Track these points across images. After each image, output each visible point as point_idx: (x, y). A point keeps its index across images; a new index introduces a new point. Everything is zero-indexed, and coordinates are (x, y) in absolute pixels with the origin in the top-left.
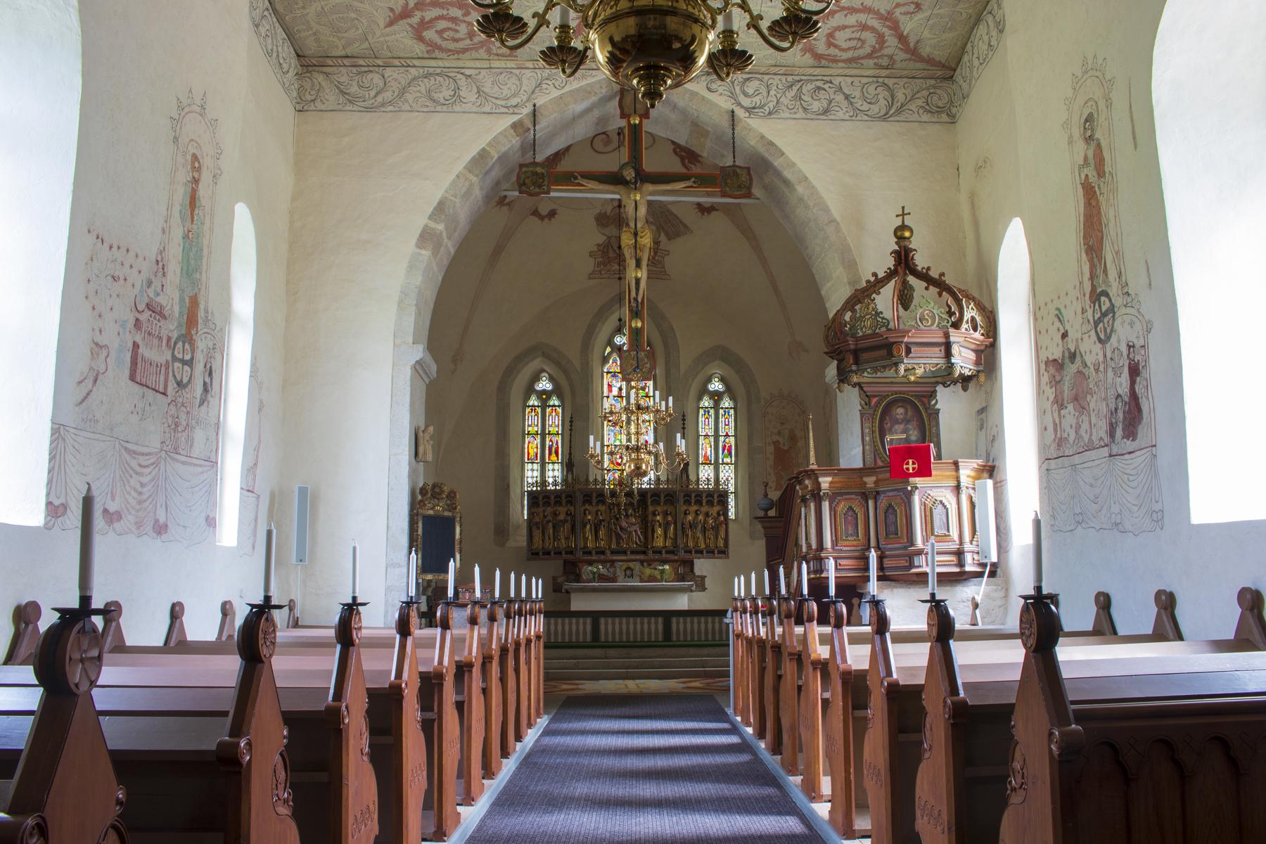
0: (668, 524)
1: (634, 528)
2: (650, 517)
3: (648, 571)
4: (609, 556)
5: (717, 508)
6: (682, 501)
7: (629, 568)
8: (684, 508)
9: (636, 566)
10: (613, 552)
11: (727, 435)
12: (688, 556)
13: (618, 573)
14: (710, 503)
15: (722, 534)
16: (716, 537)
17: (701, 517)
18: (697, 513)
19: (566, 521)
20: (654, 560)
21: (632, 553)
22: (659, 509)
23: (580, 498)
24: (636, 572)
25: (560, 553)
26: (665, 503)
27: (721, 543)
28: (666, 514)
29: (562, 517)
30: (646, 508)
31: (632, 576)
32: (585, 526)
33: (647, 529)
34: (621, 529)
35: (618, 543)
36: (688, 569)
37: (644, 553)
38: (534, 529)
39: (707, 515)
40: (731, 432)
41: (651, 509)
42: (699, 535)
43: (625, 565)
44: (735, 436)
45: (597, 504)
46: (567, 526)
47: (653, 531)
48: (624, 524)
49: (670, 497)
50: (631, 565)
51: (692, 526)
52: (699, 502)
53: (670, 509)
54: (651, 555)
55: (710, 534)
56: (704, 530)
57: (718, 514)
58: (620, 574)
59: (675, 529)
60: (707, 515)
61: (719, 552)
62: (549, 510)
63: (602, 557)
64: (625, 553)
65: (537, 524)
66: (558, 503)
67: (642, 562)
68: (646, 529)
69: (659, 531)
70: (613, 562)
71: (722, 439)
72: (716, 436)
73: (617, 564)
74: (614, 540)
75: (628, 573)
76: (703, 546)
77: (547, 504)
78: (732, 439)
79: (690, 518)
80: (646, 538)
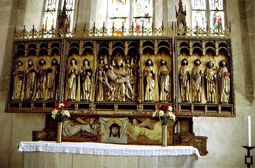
0: (162, 75)
1: (122, 80)
2: (143, 68)
3: (137, 130)
4: (93, 110)
5: (217, 60)
6: (179, 50)
7: (115, 125)
8: (181, 58)
9: (124, 123)
10: (100, 106)
11: (217, 10)
12: (186, 113)
13: (103, 130)
14: (211, 53)
15: (227, 88)
16: (219, 92)
17: (202, 68)
18: (196, 64)
19: (50, 71)
20: (145, 117)
21: (121, 107)
22: (153, 58)
23: (66, 48)
24: (124, 130)
25: (40, 105)
26: (160, 52)
27: (225, 98)
28: (161, 64)
29: (48, 66)
30: (139, 57)
31: (118, 134)
32: (70, 76)
33: (139, 81)
34: (110, 80)
35: (105, 96)
36: (185, 129)
37: (134, 108)
38: (16, 78)
39: (208, 65)
40: (221, 8)
41: (143, 58)
42: (198, 87)
43: (111, 121)
44: (225, 10)
45: (84, 54)
46: (51, 76)
47: (145, 83)
48: (113, 76)
49: (165, 46)
50: (118, 121)
51: (192, 77)
52: (198, 52)
53: (164, 58)
54: (141, 110)
55: (211, 87)
56: (205, 82)
57: (221, 64)
58: (105, 132)
59: (171, 81)
60: (208, 65)
61: (224, 109)
62: (35, 59)
63: (85, 111)
64: (111, 107)
65: (20, 72)
66: (43, 53)
67: (131, 118)
68: (138, 81)
69: (152, 84)
70: (97, 117)
71: (212, 13)
72: (208, 11)
73: (102, 120)
74: (101, 92)
75: (114, 130)
76: (204, 101)
77: (32, 53)
78: (221, 14)
79: (188, 68)
80: (137, 91)
